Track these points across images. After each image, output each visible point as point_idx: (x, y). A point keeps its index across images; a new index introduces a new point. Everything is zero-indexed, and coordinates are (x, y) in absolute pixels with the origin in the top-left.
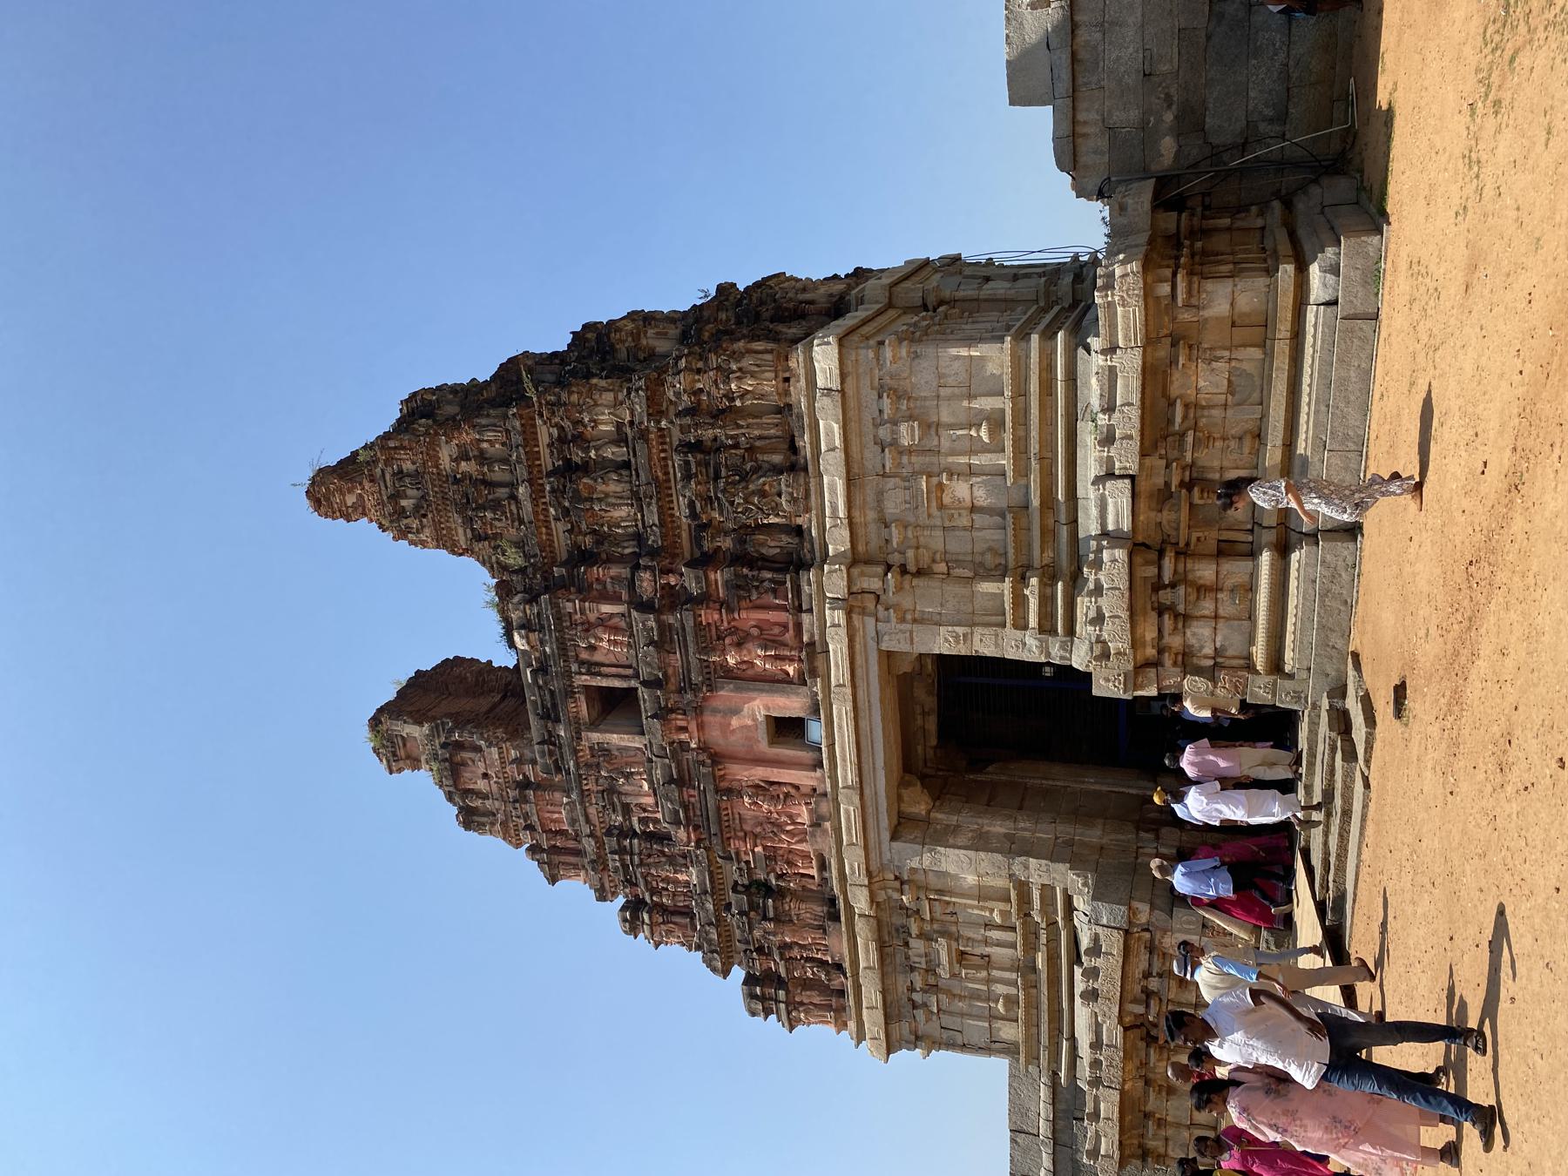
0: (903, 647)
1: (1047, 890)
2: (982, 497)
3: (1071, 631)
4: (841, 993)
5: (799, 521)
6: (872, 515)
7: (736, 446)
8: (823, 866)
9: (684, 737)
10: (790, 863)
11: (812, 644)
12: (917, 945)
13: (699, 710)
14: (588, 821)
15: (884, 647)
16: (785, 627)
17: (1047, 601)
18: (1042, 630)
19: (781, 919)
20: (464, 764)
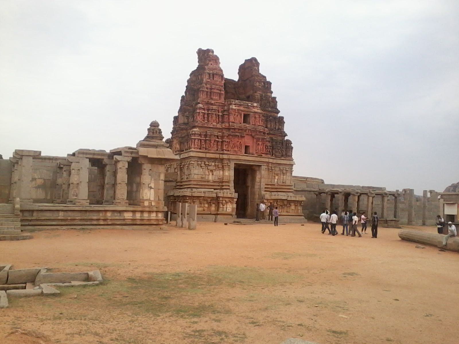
0: (262, 169)
1: (229, 186)
2: (276, 180)
3: (265, 191)
4: (200, 149)
5: (274, 155)
6: (275, 166)
7: (283, 148)
8: (226, 150)
9: (247, 132)
10: (226, 145)
11: (262, 155)
12: (213, 164)
13: (251, 135)
14: (216, 103)
15: (262, 166)
16: (263, 151)
17: (267, 188)
18: (265, 187)
19: (215, 141)
20: (219, 76)
